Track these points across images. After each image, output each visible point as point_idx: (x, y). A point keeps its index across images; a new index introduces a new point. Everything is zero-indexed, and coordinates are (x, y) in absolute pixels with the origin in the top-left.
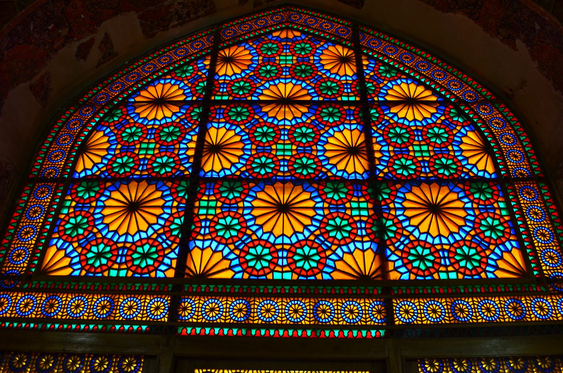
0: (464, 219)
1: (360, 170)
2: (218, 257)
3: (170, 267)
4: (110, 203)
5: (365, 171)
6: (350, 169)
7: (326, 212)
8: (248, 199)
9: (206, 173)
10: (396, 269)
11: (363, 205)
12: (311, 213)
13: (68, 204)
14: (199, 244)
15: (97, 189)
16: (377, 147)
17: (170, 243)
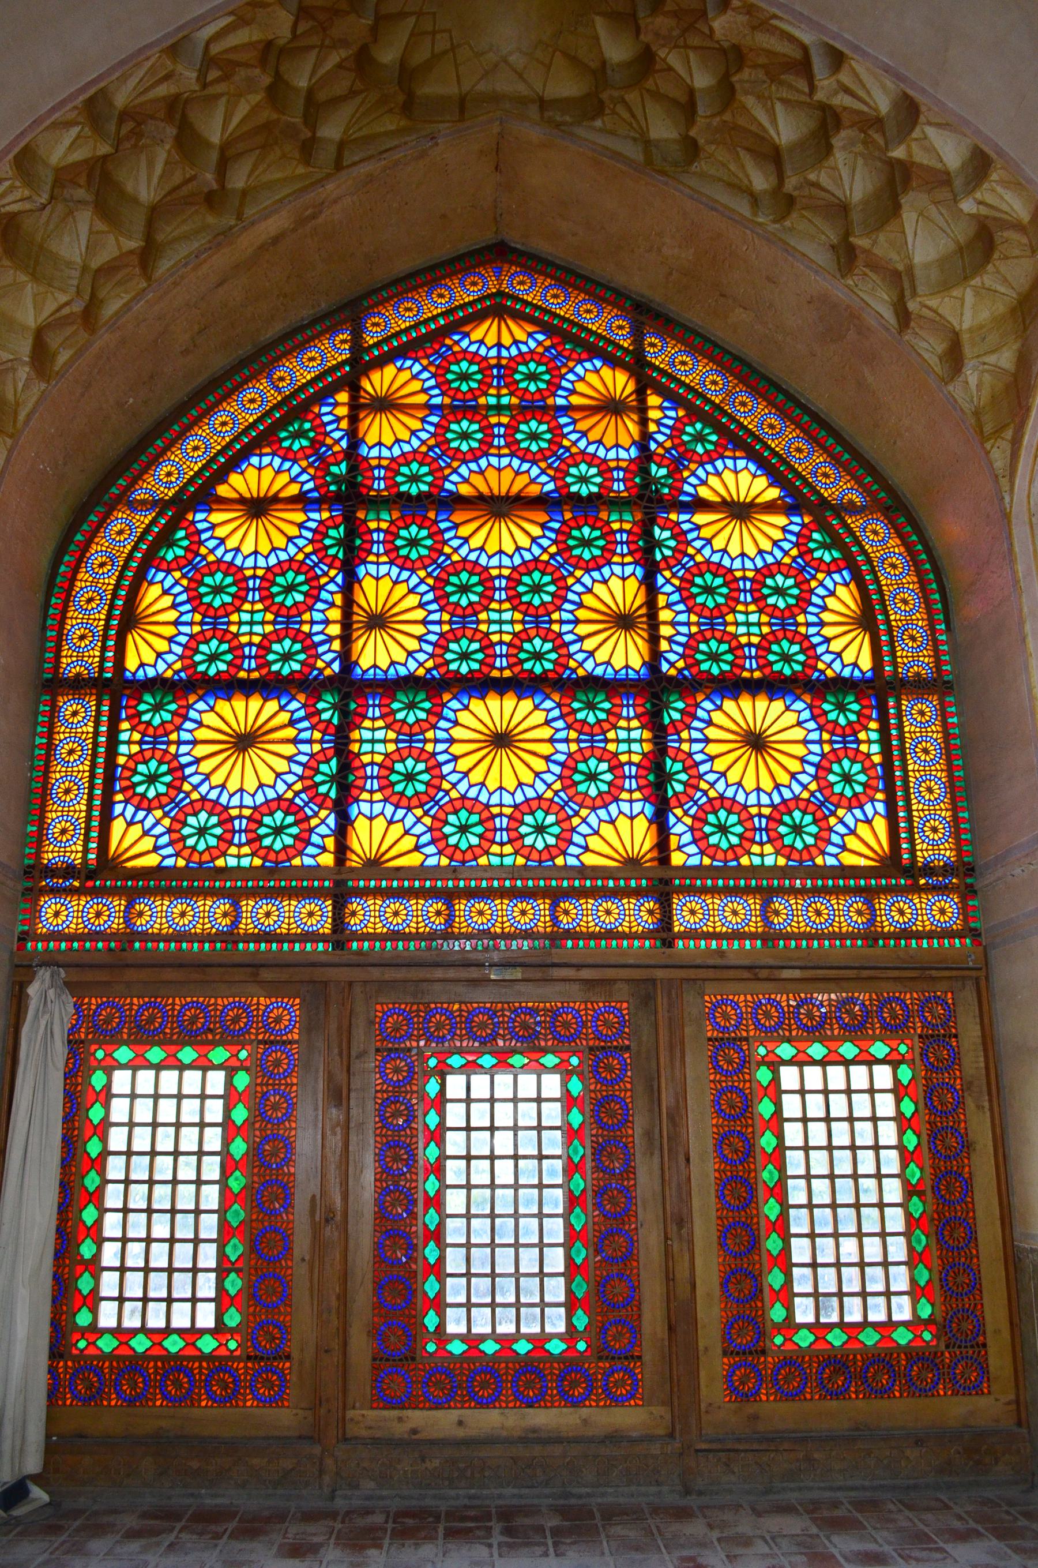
0: (802, 760)
1: (636, 662)
2: (397, 830)
3: (324, 849)
4: (202, 734)
5: (644, 664)
6: (618, 662)
7: (574, 747)
8: (443, 724)
9: (365, 672)
10: (679, 848)
11: (635, 734)
12: (546, 749)
13: (124, 736)
14: (365, 807)
15: (173, 707)
16: (665, 615)
17: (316, 809)
